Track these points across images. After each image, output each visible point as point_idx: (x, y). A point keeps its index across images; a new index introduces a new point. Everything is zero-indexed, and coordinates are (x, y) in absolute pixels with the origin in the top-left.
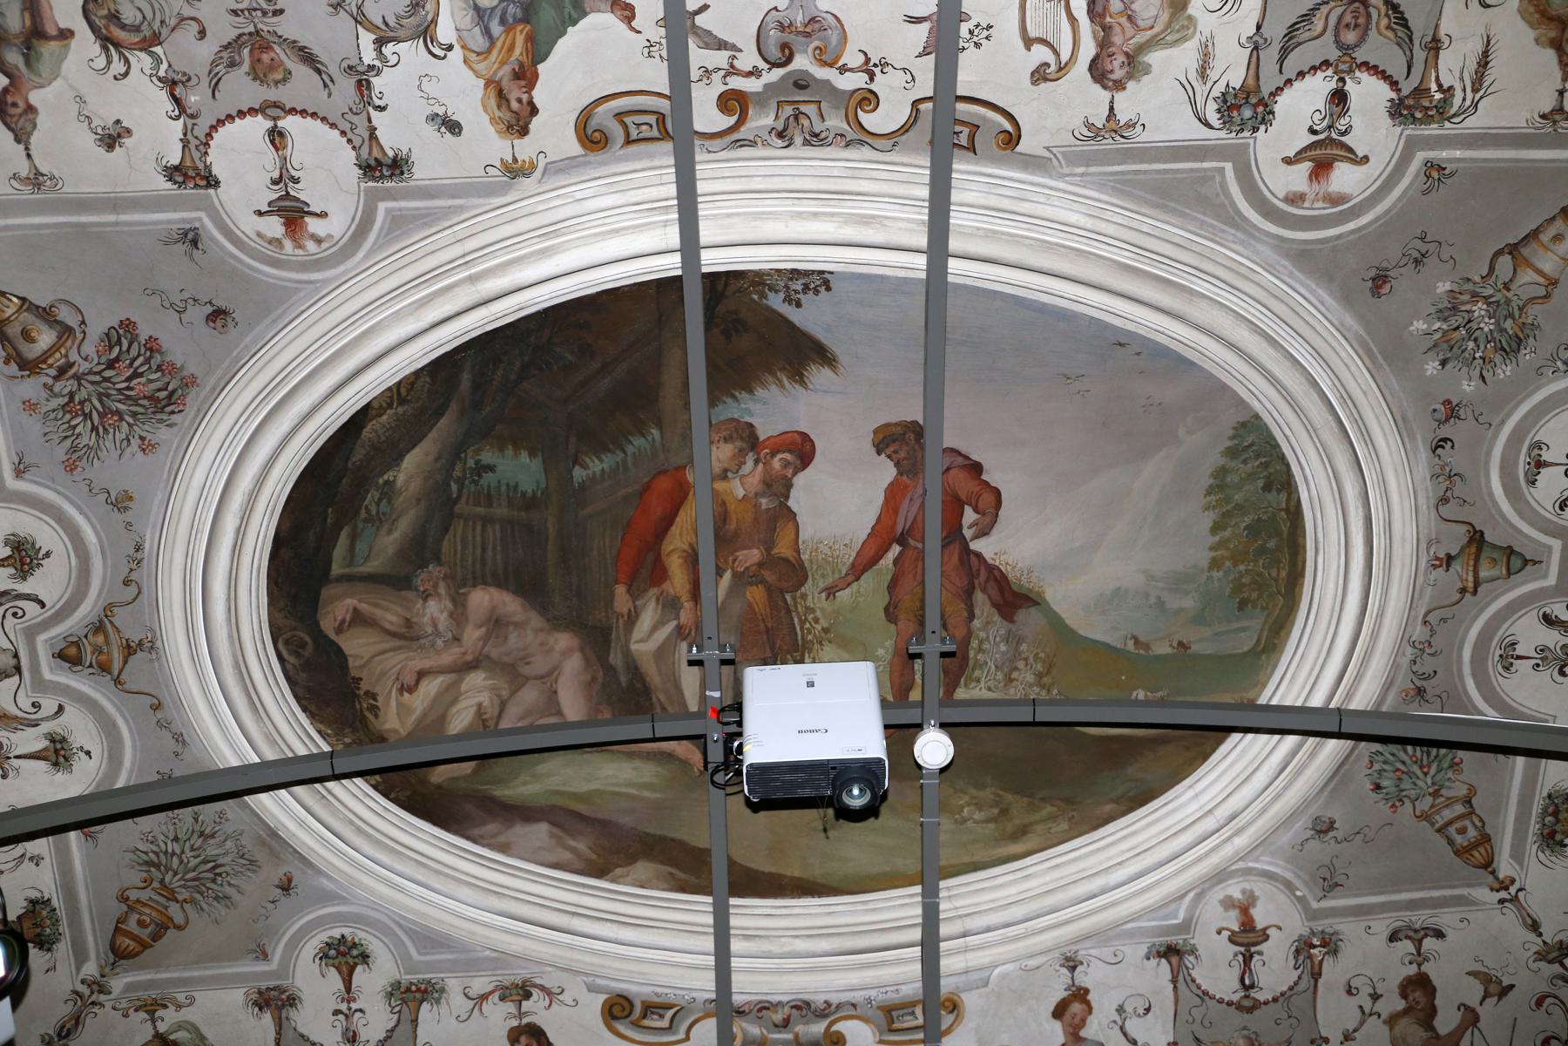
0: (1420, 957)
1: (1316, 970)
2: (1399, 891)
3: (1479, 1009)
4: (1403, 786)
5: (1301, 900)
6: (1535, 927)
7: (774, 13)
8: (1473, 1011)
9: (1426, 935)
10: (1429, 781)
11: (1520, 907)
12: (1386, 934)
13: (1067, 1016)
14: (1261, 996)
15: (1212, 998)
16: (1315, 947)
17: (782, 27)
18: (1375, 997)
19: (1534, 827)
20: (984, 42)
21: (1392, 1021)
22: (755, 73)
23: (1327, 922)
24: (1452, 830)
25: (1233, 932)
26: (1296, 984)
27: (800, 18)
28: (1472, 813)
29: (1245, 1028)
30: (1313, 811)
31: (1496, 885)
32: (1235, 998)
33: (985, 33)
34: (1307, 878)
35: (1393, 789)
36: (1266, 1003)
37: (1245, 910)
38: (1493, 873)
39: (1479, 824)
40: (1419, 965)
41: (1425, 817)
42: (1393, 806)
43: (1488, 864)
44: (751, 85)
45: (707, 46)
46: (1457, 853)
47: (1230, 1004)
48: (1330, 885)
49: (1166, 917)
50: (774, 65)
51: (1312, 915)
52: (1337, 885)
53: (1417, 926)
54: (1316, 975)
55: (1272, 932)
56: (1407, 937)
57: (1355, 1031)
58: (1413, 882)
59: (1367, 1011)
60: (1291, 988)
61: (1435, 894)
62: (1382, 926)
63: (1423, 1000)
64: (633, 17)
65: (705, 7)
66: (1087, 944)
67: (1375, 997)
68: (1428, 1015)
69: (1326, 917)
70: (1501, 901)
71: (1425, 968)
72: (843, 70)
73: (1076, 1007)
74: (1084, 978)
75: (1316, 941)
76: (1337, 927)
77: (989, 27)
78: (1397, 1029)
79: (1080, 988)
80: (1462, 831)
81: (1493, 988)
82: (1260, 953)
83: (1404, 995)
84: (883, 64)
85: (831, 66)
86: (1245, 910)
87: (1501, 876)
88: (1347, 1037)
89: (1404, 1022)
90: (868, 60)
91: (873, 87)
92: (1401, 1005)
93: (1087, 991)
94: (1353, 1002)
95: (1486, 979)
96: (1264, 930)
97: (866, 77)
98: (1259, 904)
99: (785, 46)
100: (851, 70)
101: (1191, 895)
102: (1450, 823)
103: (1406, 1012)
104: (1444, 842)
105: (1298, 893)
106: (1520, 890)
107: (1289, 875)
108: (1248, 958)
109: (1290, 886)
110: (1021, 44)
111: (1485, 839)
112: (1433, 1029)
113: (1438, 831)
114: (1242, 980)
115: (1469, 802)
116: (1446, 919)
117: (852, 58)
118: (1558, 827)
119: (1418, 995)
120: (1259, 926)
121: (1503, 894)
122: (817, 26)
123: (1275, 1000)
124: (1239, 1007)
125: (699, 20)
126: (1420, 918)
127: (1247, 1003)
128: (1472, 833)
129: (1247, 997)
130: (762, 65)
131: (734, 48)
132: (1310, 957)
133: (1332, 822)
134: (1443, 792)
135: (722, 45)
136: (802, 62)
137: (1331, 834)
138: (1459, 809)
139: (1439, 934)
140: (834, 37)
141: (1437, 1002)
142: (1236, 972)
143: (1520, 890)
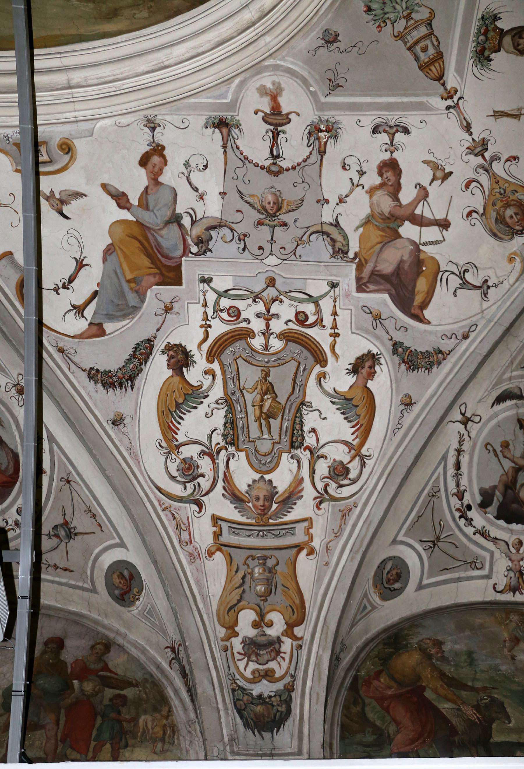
0: (392, 147)
1: (322, 149)
2: (381, 96)
3: (429, 188)
4: (386, 10)
5: (313, 94)
6: (468, 128)
8: (425, 189)
9: (397, 131)
10: (404, 7)
11: (460, 113)
12: (370, 128)
13: (150, 166)
14: (284, 164)
15: (251, 162)
16: (322, 131)
18: (361, 173)
19: (471, 46)
21: (371, 192)
23: (332, 113)
24: (418, 48)
25: (266, 114)
26: (308, 157)
28: (432, 34)
29: (273, 187)
30: (323, 25)
31: (445, 95)
32: (267, 164)
34: (317, 77)
35: (379, 12)
36: (287, 170)
37: (274, 98)
38: (443, 84)
39: (436, 43)
40: (392, 152)
41: (400, 37)
42: (379, 26)
43: (440, 78)
46: (421, 68)
47: (263, 168)
48: (334, 86)
49: (219, 97)
51: (321, 107)
52: (339, 86)
53: (392, 124)
54: (322, 153)
55: (292, 116)
56: (385, 131)
57: (347, 196)
58: (392, 90)
59: (355, 183)
60: (305, 161)
61: (405, 99)
62: (369, 120)
63: (393, 179)
66: (163, 110)
67: (361, 173)
68: (395, 190)
69: (330, 110)
70: (448, 108)
71: (395, 155)
73: (156, 159)
74: (164, 137)
75: (322, 127)
76: (338, 118)
78: (375, 198)
79: (158, 145)
80: (425, 49)
81: (439, 174)
82: (284, 132)
83: (381, 174)
86: (274, 98)
87: (449, 88)
88: (341, 200)
89: (379, 193)
92: (378, 180)
93: (163, 148)
94: (347, 175)
95: (435, 167)
96: (288, 114)
98: (284, 93)
101: (237, 81)
102: (416, 43)
103: (381, 186)
104: (411, 58)
105: (312, 89)
106: (460, 98)
107: (306, 74)
108: (276, 135)
109: (305, 82)
111: (439, 56)
112: (398, 200)
113: (409, 49)
114: (271, 151)
115: (430, 24)
116: (411, 120)
118: (487, 45)
119: (389, 174)
120: (284, 112)
121: (449, 102)
123: (294, 168)
124: (269, 171)
126: (394, 117)
127: (274, 169)
128: (431, 51)
129: (274, 164)
132: (318, 138)
133: (337, 35)
134: (413, 15)
137: (336, 45)
138: (423, 30)
139: (406, 131)
141: (402, 181)
142: (267, 144)
143: (460, 98)
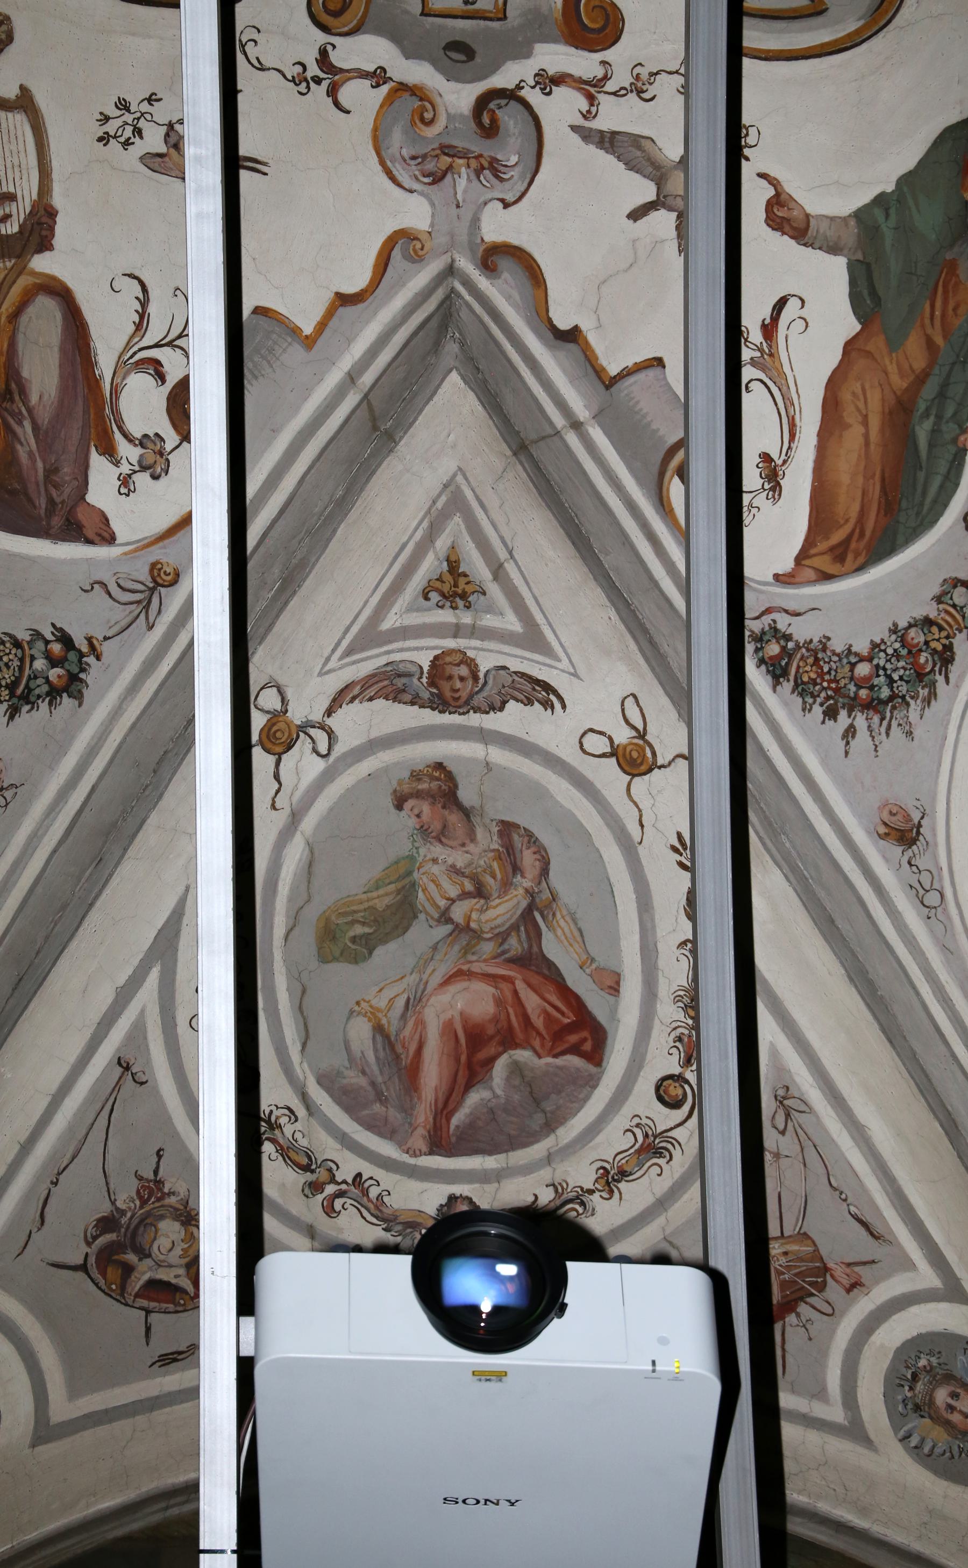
7: (510, 198)
17: (495, 168)
20: (112, 111)
22: (549, 82)
27: (462, 183)
33: (111, 127)
44: (556, 57)
45: (636, 140)
50: (511, 95)
64: (770, 205)
65: (636, 215)
72: (378, 77)
77: (104, 139)
84: (301, 80)
85: (403, 88)
90: (332, 92)
91: (321, 38)
97: (336, 58)
99: (490, 131)
100: (363, 75)
110: (42, 100)
117: (362, 97)
122: (430, 166)
125: (649, 192)
130: (533, 97)
131: (586, 135)
135: (609, 141)
136: (457, 97)
140: (397, 140)
